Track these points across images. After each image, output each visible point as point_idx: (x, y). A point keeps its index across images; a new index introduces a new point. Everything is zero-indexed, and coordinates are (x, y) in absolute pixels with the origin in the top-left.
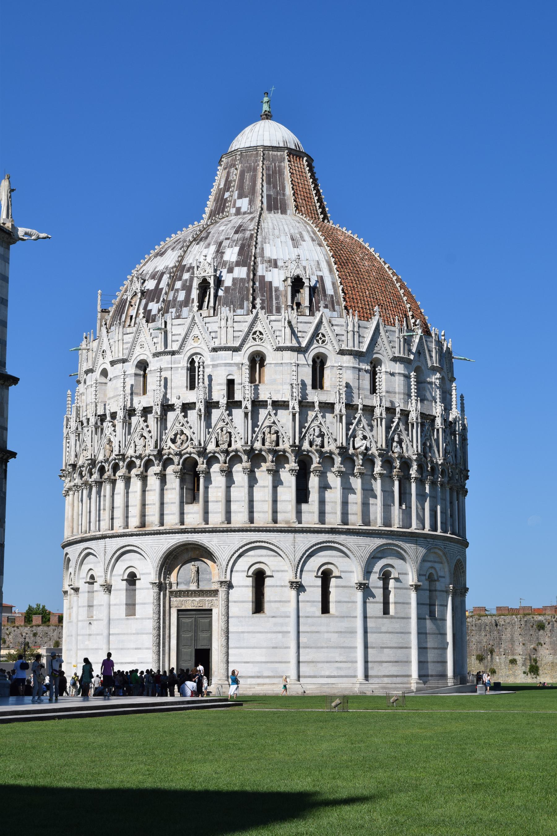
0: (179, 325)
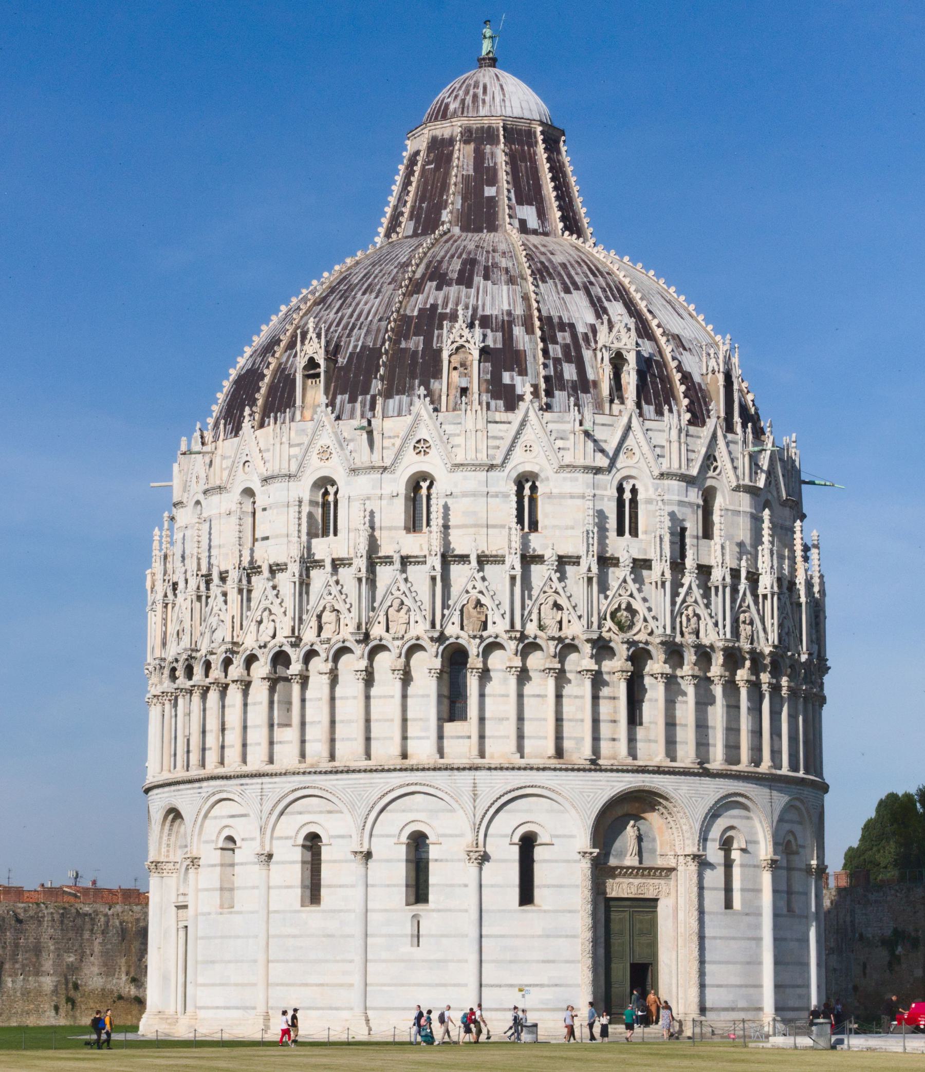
0: (603, 425)
